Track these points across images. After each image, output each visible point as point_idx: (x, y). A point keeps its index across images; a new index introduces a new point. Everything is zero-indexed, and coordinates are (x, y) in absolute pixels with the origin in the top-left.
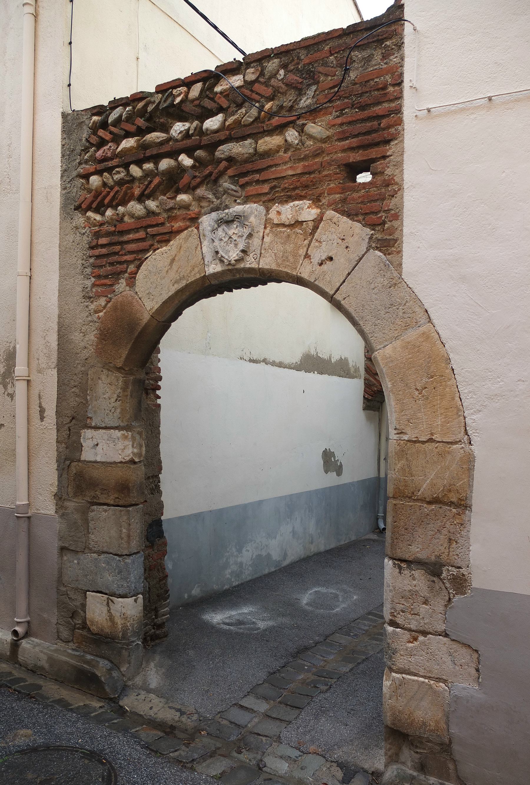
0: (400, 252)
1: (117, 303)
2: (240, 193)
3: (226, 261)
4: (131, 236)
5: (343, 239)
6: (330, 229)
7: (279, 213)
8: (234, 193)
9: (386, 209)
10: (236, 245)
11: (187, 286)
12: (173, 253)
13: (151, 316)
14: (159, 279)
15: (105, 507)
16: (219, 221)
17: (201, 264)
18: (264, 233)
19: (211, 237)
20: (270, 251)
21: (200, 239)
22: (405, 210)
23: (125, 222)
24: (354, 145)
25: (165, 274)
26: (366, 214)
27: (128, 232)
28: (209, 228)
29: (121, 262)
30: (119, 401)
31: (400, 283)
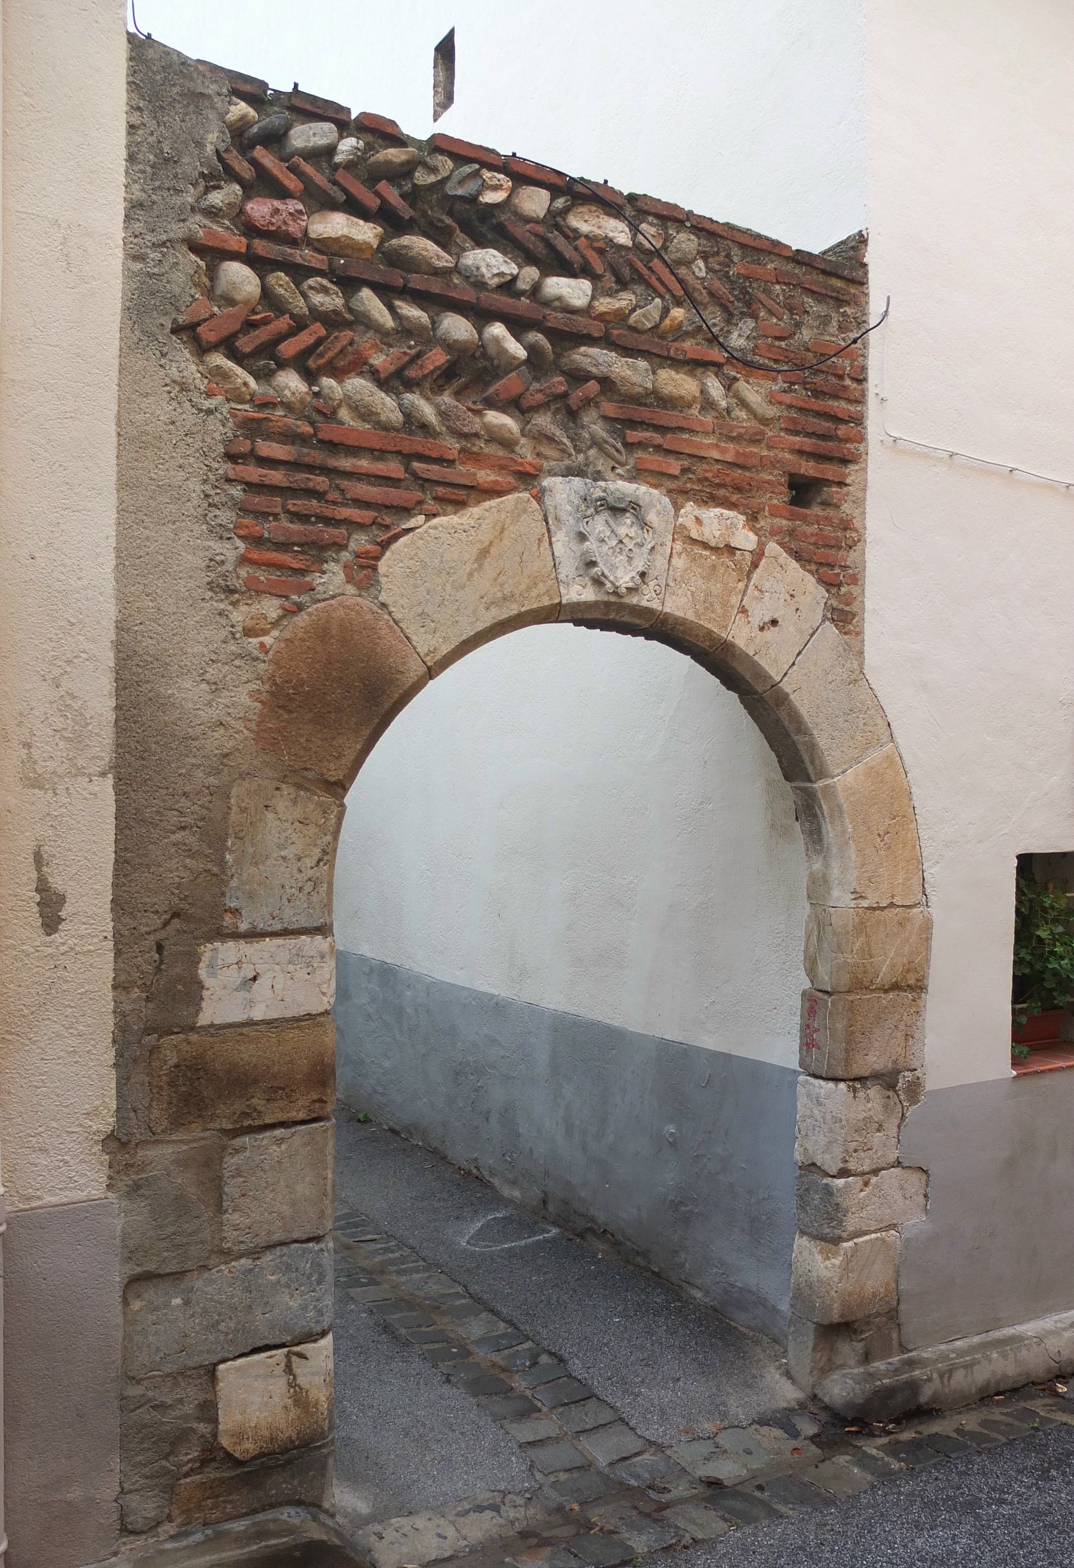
0: (859, 633)
1: (328, 622)
3: (609, 585)
4: (364, 464)
5: (792, 596)
6: (775, 574)
7: (698, 521)
8: (616, 453)
9: (843, 564)
10: (630, 559)
12: (486, 535)
14: (449, 586)
15: (279, 1132)
16: (599, 503)
21: (547, 523)
22: (868, 573)
23: (343, 424)
24: (807, 449)
25: (465, 578)
26: (821, 564)
27: (355, 451)
28: (569, 508)
29: (333, 519)
30: (325, 864)
31: (861, 679)
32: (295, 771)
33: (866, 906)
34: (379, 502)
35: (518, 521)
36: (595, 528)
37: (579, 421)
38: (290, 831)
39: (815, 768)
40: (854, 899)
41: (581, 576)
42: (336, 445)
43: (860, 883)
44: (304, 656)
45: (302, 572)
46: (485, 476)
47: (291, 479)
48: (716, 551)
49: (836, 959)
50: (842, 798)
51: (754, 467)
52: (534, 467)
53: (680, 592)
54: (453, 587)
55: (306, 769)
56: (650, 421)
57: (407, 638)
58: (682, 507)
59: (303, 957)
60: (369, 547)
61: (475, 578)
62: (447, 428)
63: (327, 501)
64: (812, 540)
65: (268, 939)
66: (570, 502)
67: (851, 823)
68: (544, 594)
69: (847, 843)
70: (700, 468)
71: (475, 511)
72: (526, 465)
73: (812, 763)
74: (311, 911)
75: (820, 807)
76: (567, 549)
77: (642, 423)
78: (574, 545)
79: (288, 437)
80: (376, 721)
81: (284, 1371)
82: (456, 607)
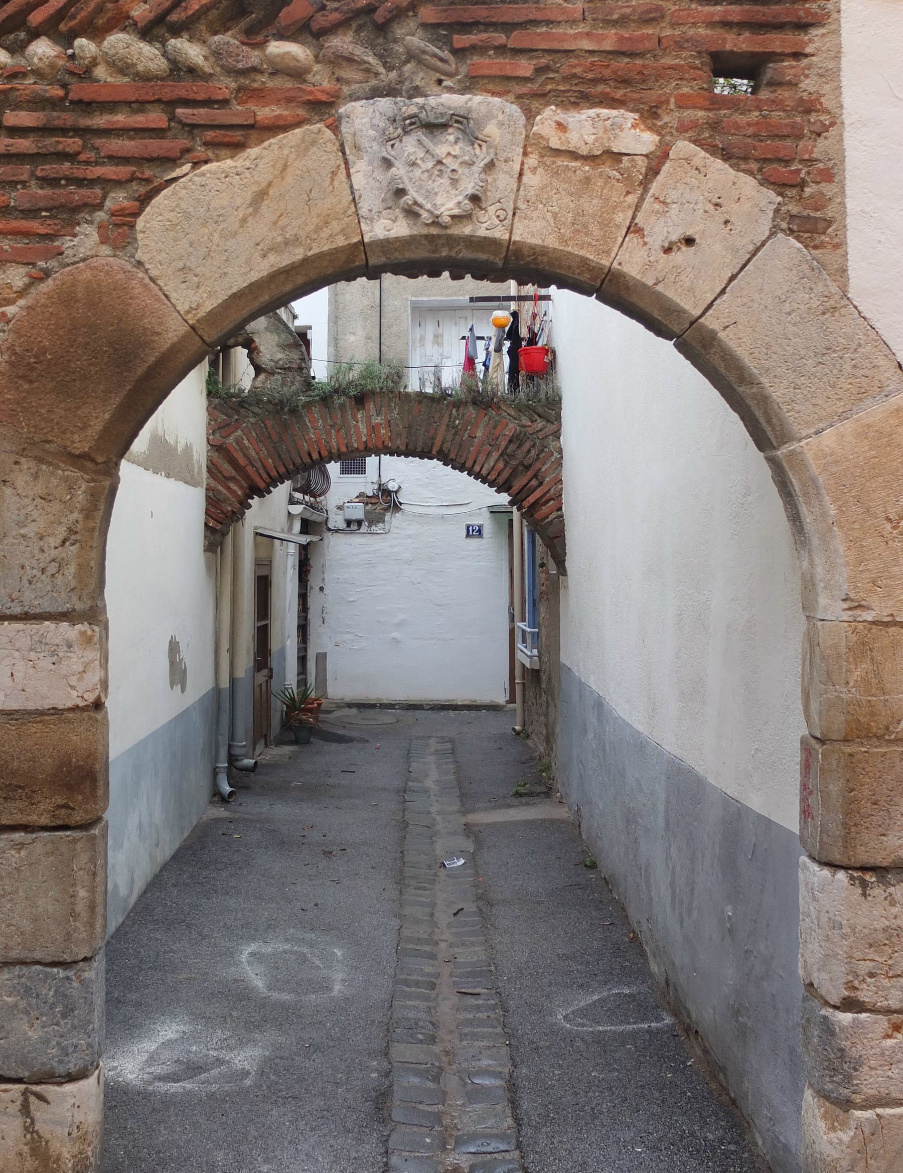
0: (839, 245)
1: (73, 285)
2: (454, 66)
3: (425, 215)
4: (121, 119)
5: (717, 205)
6: (688, 180)
7: (561, 127)
8: (439, 64)
9: (806, 157)
10: (454, 182)
11: (306, 261)
12: (263, 175)
13: (192, 327)
14: (216, 235)
15: (18, 836)
16: (408, 122)
17: (350, 212)
18: (522, 164)
19: (384, 154)
20: (541, 206)
21: (344, 153)
22: (848, 165)
23: (98, 81)
24: (736, 18)
25: (237, 225)
26: (765, 160)
27: (111, 106)
28: (372, 133)
29: (85, 179)
30: (73, 544)
31: (845, 306)
32: (34, 444)
33: (870, 619)
34: (136, 155)
35: (305, 155)
36: (404, 151)
37: (390, 36)
38: (30, 508)
39: (773, 429)
40: (850, 609)
41: (390, 208)
42: (89, 104)
43: (856, 587)
44: (47, 323)
45: (50, 237)
46: (266, 112)
47: (40, 145)
48: (593, 161)
49: (826, 693)
50: (814, 468)
51: (649, 51)
52: (328, 94)
53: (535, 215)
54: (221, 236)
55: (49, 442)
56: (487, 20)
57: (166, 296)
58: (539, 113)
59: (46, 644)
60: (126, 203)
61: (249, 224)
62: (222, 67)
63: (79, 162)
64: (750, 131)
65: (6, 623)
66: (373, 126)
67: (834, 502)
68: (338, 234)
69: (830, 530)
70: (566, 66)
71: (253, 152)
72: (317, 93)
73: (769, 421)
74: (55, 595)
75: (791, 482)
76: (371, 180)
77: (476, 24)
78: (379, 175)
79: (38, 103)
80: (128, 387)
81: (20, 1110)
82: (225, 258)
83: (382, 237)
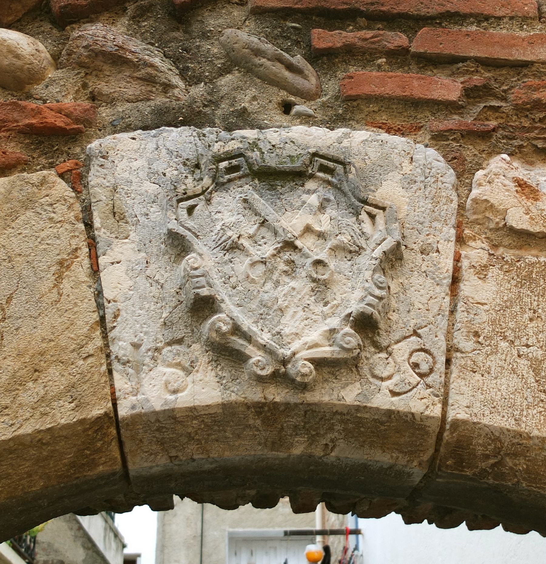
2: (313, 80)
8: (287, 74)
17: (90, 348)
18: (457, 259)
19: (173, 225)
20: (504, 345)
21: (89, 226)
28: (151, 188)
37: (196, 27)
41: (179, 342)
53: (494, 362)
58: (479, 166)
68: (58, 397)
83: (158, 408)
